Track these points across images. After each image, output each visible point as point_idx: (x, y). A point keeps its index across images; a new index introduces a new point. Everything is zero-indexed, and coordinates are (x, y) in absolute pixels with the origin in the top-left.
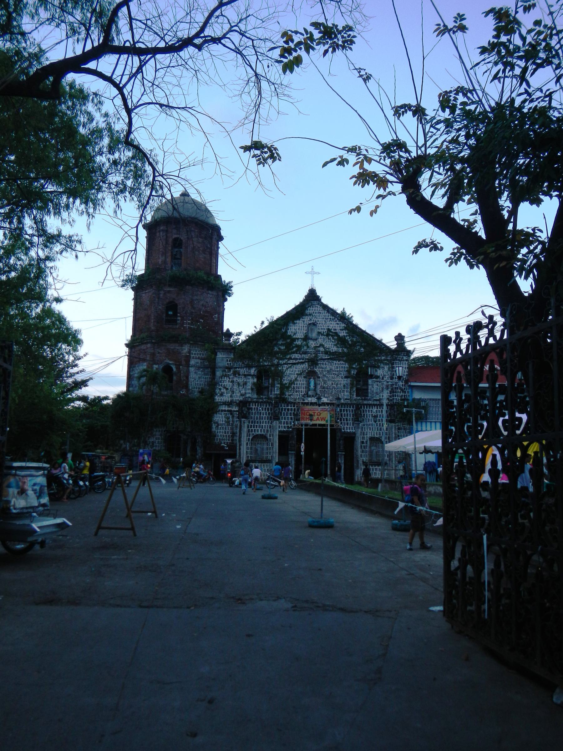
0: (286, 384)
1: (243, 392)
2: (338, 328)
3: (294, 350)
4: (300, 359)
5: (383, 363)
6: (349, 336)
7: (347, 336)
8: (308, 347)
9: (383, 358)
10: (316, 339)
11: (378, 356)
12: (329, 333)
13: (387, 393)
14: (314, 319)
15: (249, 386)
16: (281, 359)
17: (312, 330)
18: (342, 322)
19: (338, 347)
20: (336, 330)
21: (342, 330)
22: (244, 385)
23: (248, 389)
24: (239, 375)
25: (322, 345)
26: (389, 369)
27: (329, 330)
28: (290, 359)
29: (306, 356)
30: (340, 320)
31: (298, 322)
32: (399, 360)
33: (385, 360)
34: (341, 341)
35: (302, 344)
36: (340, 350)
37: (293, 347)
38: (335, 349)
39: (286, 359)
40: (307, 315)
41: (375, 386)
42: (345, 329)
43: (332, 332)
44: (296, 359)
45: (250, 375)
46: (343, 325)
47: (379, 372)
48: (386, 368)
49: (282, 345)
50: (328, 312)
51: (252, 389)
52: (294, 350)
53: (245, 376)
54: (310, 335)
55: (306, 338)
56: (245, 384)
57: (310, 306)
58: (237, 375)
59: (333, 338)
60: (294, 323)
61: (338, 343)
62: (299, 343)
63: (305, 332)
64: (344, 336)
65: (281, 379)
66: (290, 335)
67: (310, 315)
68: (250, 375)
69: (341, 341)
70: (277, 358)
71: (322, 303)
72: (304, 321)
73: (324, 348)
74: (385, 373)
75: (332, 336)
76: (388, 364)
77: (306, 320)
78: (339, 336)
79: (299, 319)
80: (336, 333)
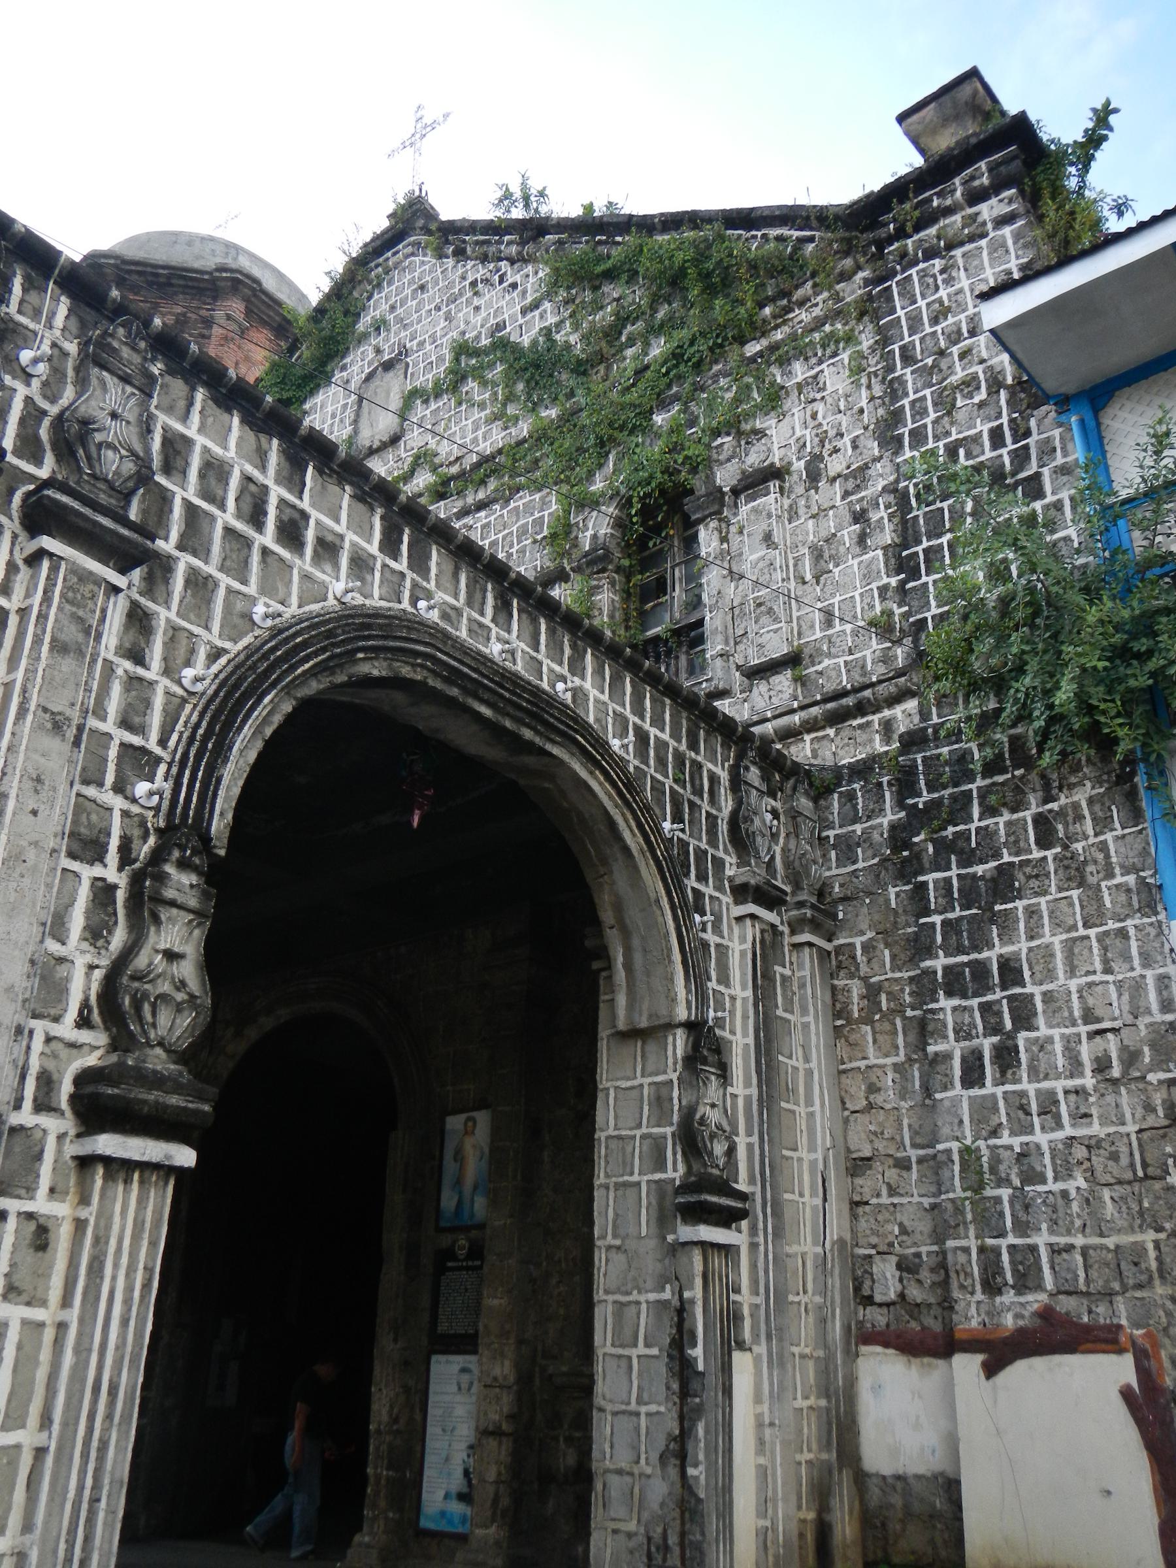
5: (802, 353)
7: (559, 325)
9: (803, 316)
11: (761, 329)
13: (868, 575)
14: (388, 343)
21: (535, 305)
26: (857, 370)
27: (462, 349)
32: (930, 254)
33: (818, 324)
38: (494, 439)
41: (752, 555)
42: (554, 285)
47: (782, 437)
48: (835, 379)
50: (460, 254)
57: (379, 286)
59: (484, 383)
61: (510, 398)
64: (547, 332)
69: (534, 369)
74: (827, 420)
76: (850, 339)
77: (355, 368)
78: (516, 349)
79: (327, 379)
80: (502, 346)
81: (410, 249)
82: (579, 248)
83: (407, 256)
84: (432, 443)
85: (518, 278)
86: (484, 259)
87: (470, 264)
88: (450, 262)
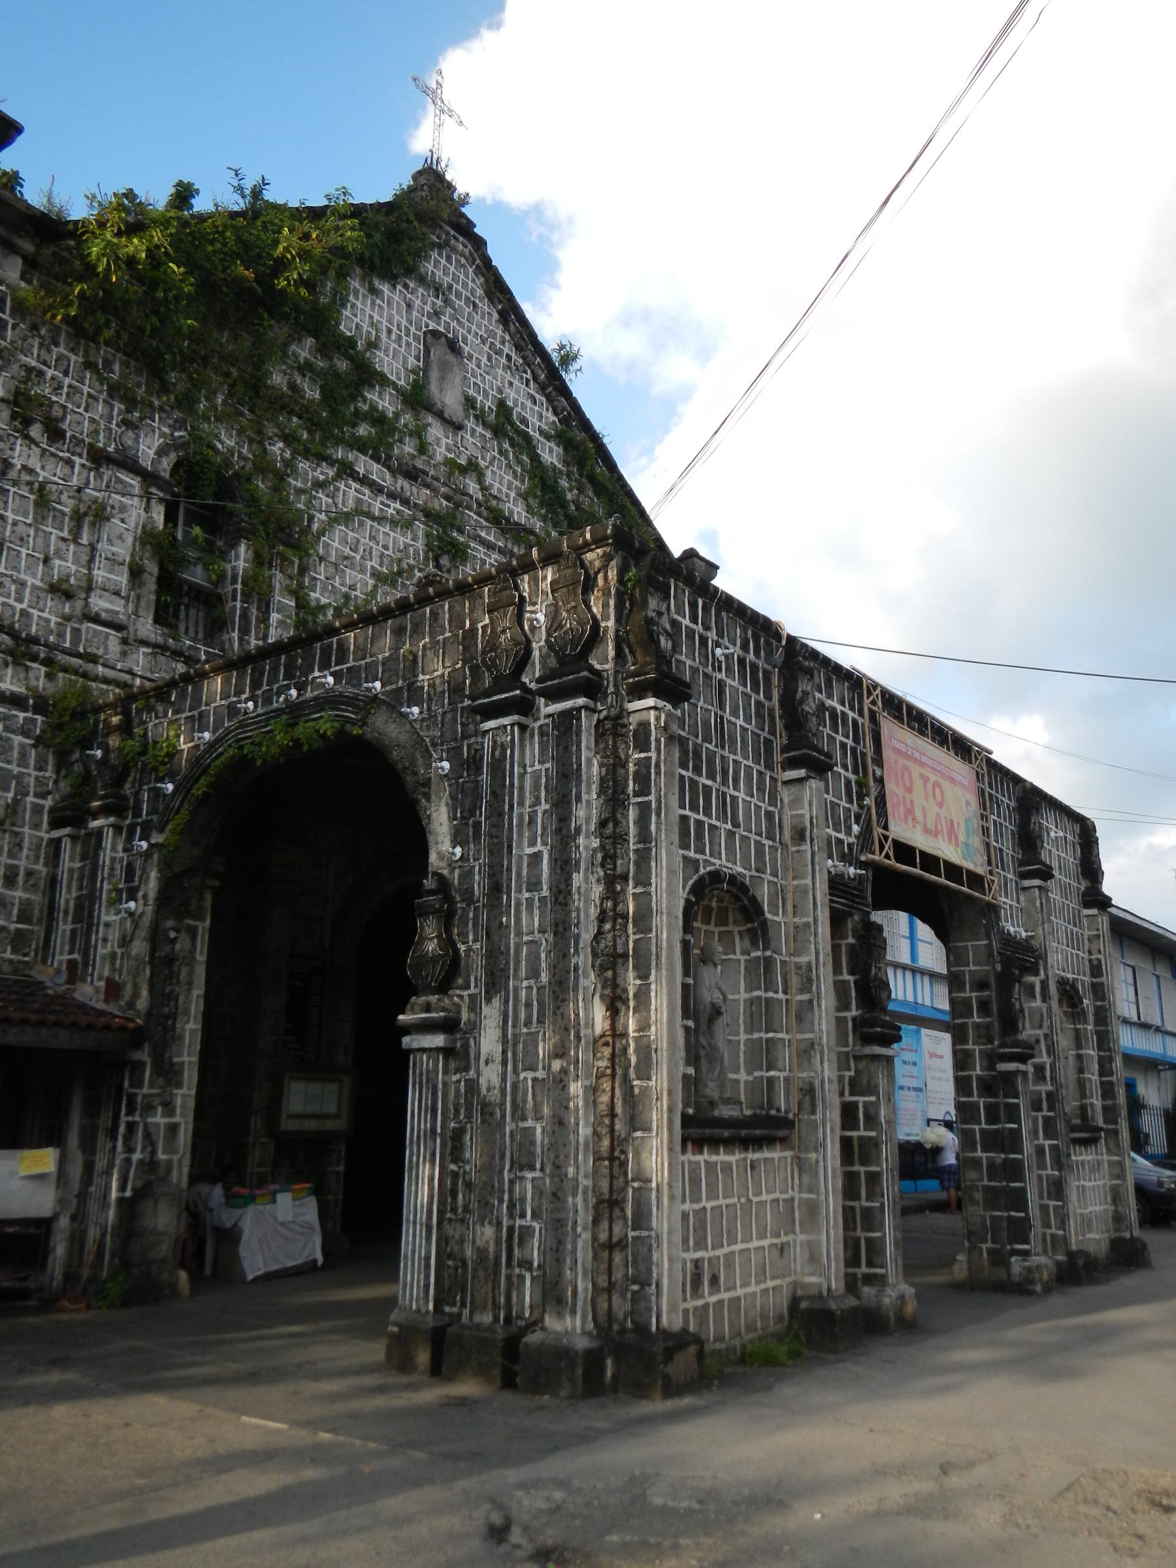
0: (322, 608)
1: (67, 565)
2: (533, 420)
3: (363, 430)
4: (392, 496)
6: (569, 475)
8: (422, 449)
10: (458, 427)
12: (503, 424)
15: (120, 538)
16: (307, 454)
17: (445, 368)
18: (548, 397)
19: (529, 509)
20: (524, 421)
21: (548, 437)
22: (78, 518)
23: (113, 562)
24: (55, 433)
25: (472, 467)
28: (346, 471)
29: (420, 495)
30: (542, 389)
31: (385, 288)
34: (542, 487)
35: (397, 415)
36: (538, 525)
37: (358, 416)
38: (518, 512)
39: (331, 462)
40: (422, 280)
43: (512, 424)
44: (377, 489)
45: (129, 464)
46: (552, 418)
49: (305, 368)
50: (504, 319)
51: (136, 573)
52: (363, 430)
53: (98, 458)
54: (434, 388)
55: (417, 398)
56: (99, 515)
58: (36, 431)
60: (373, 291)
62: (386, 403)
63: (412, 362)
65: (303, 570)
66: (352, 342)
67: (438, 289)
68: (129, 464)
70: (289, 439)
71: (487, 261)
72: (409, 306)
73: (484, 489)
75: (511, 440)
81: (466, 251)
82: (579, 436)
83: (462, 255)
84: (482, 463)
85: (537, 396)
86: (519, 348)
87: (507, 337)
88: (496, 316)
